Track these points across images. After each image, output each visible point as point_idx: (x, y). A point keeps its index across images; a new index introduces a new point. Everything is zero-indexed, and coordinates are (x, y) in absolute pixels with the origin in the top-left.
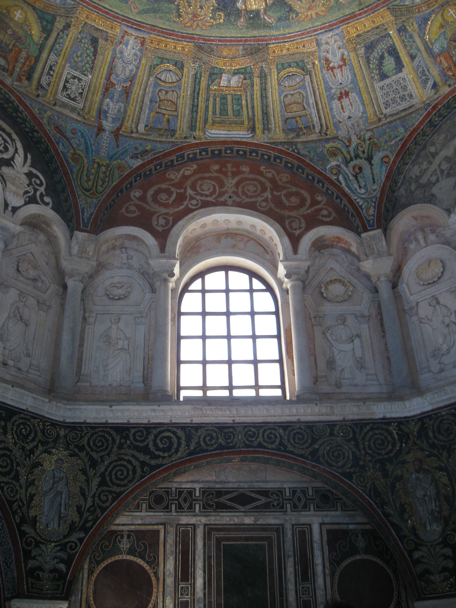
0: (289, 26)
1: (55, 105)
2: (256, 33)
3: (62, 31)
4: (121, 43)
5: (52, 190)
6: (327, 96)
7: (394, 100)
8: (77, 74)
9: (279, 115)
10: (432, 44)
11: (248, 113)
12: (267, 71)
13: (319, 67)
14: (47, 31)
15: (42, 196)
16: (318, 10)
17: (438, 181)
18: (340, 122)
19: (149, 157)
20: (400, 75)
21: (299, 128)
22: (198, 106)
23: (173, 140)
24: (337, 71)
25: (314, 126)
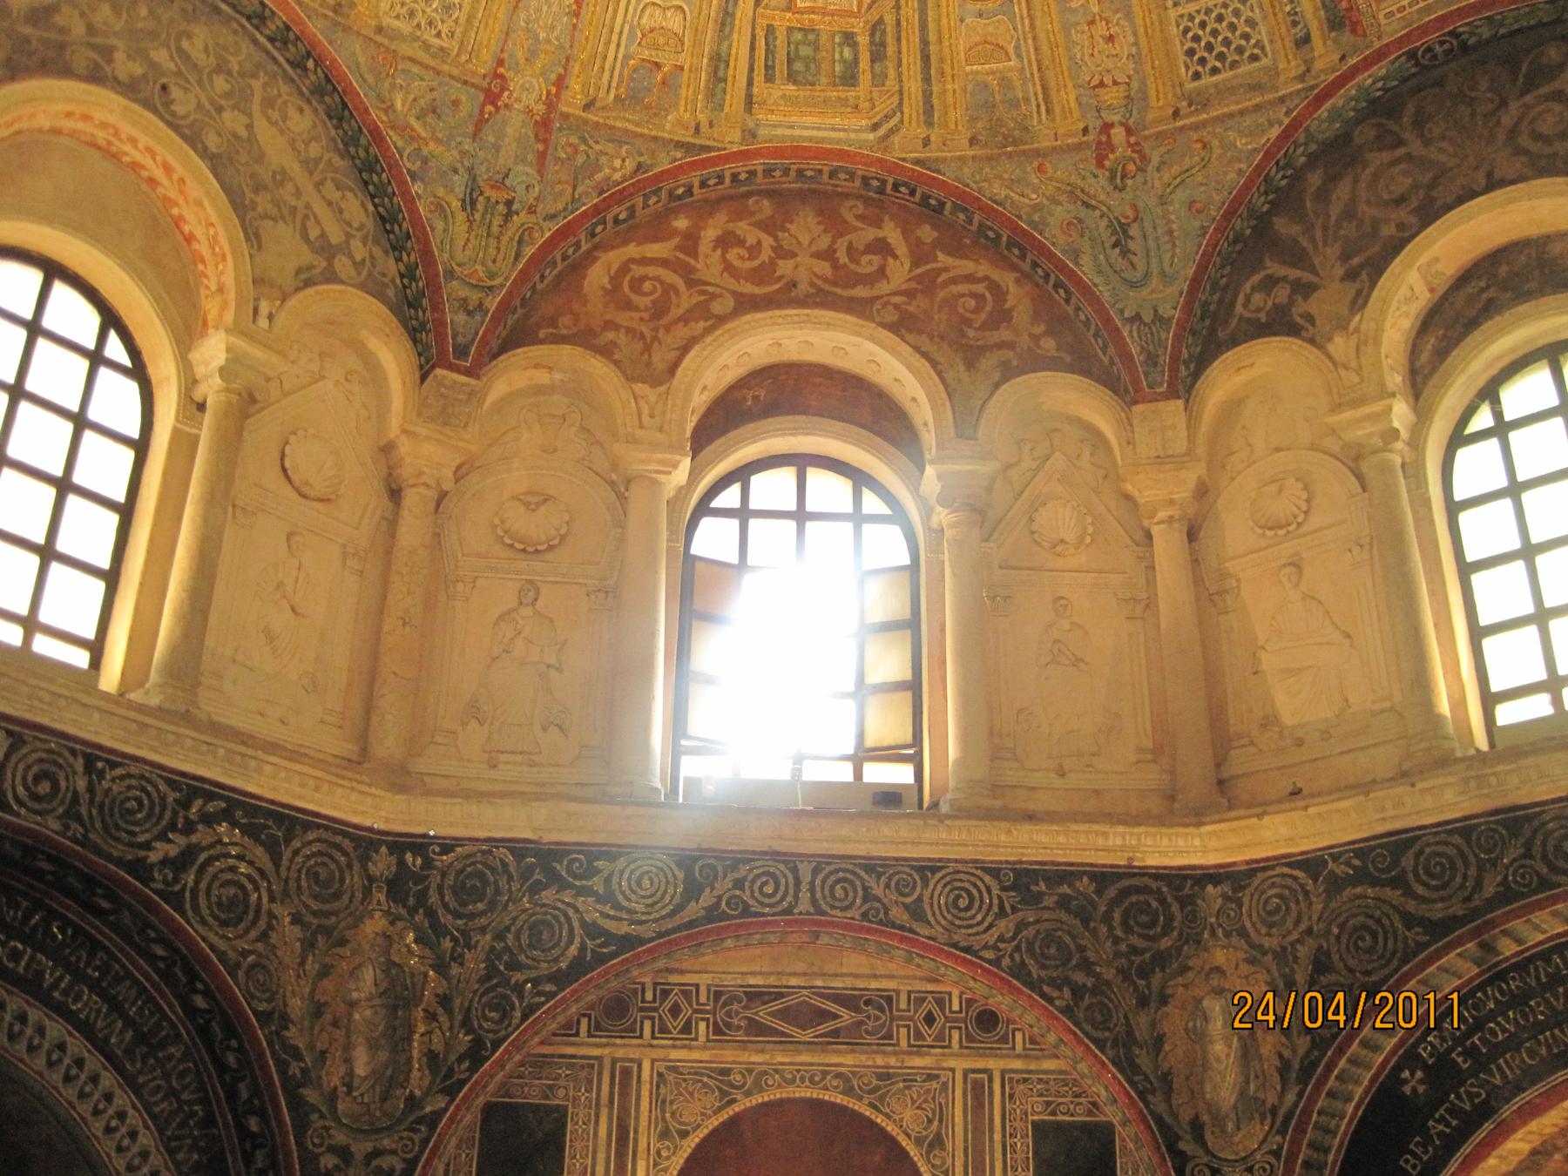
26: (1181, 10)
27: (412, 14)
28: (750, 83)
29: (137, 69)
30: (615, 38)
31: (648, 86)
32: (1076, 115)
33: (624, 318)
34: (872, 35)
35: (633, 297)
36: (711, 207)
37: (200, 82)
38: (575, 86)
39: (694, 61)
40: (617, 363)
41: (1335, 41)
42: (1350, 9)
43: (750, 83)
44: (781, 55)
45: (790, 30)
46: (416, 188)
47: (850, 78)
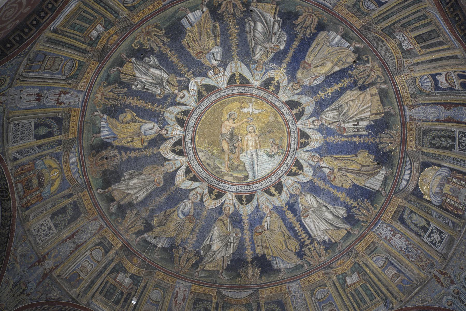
6: (44, 87)
7: (18, 130)
9: (52, 52)
10: (42, 160)
11: (68, 32)
12: (86, 55)
13: (66, 87)
16: (98, 99)
18: (21, 91)
21: (34, 62)
22: (99, 4)
24: (56, 97)
25: (29, 72)
27: (38, 231)
28: (96, 292)
30: (75, 264)
31: (74, 279)
34: (127, 295)
39: (87, 279)
43: (96, 292)
45: (112, 284)
47: (117, 303)
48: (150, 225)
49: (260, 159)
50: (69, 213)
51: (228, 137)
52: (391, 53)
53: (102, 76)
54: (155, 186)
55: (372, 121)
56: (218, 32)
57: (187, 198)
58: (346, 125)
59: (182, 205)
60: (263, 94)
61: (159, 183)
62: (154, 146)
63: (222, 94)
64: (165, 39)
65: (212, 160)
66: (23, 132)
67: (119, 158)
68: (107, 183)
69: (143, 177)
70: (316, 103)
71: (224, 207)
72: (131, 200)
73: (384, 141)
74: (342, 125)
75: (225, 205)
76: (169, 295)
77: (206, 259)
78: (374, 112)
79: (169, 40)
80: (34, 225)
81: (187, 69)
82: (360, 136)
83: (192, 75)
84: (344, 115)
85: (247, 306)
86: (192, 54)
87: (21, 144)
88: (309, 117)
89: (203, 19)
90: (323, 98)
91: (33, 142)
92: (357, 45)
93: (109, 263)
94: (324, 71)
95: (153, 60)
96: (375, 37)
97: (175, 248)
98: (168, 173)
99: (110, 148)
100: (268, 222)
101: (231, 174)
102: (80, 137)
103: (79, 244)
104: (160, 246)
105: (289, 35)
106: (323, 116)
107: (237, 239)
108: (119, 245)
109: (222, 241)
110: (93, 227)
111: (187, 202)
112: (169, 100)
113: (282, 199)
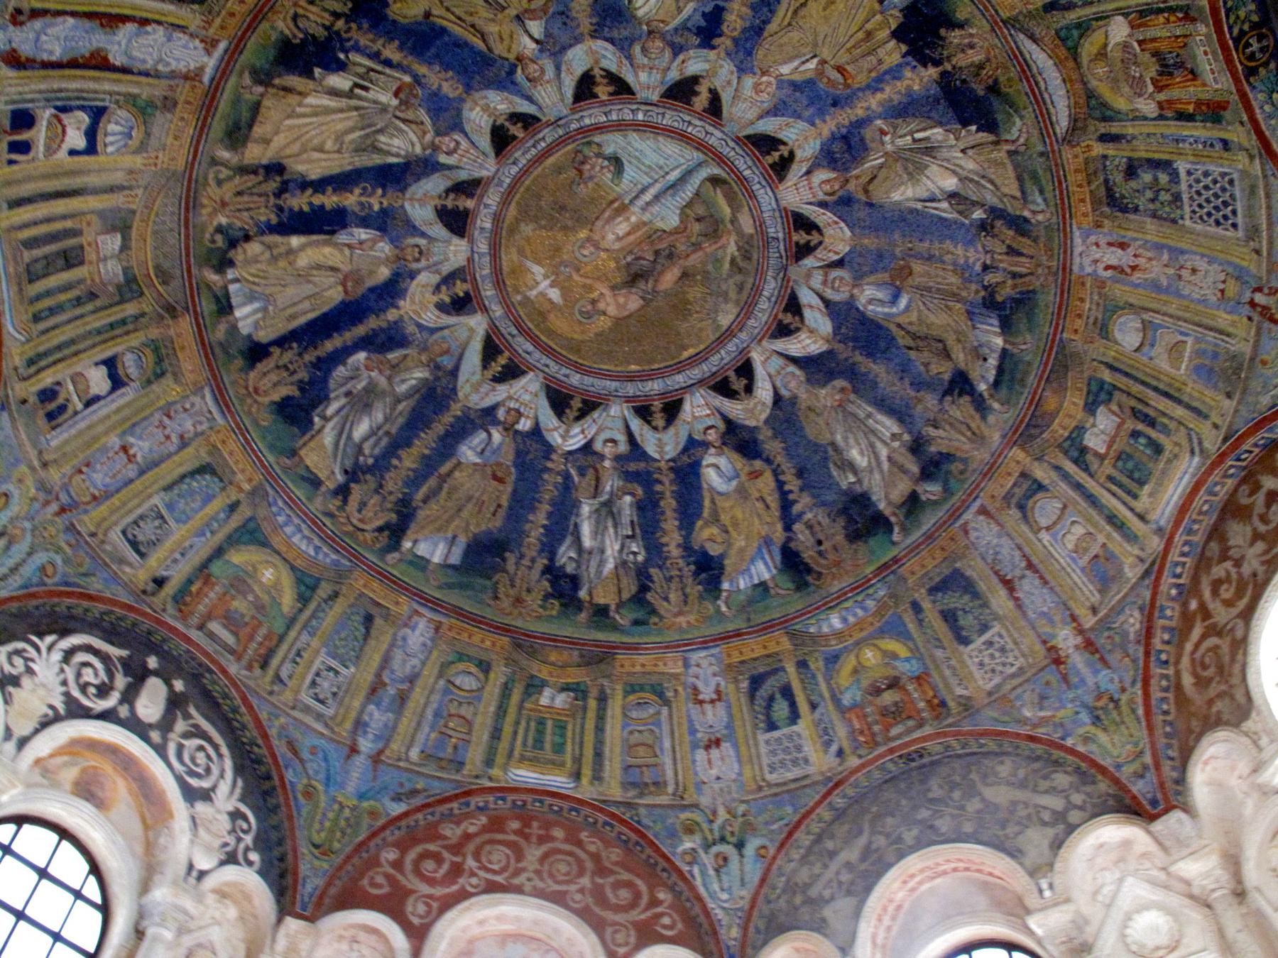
0: (648, 634)
1: (293, 708)
2: (601, 636)
3: (325, 601)
4: (406, 625)
5: (262, 843)
8: (334, 663)
14: (304, 600)
15: (247, 849)
16: (692, 618)
17: (832, 898)
19: (418, 801)
20: (795, 728)
23: (458, 777)
24: (708, 707)
25: (665, 783)
26: (1187, 216)
27: (993, 671)
29: (915, 832)
31: (1102, 570)
32: (1236, 318)
33: (1213, 690)
35: (1206, 674)
36: (1195, 579)
37: (947, 806)
38: (1082, 612)
40: (1227, 723)
41: (1229, 123)
42: (1208, 106)
43: (1132, 510)
44: (1125, 480)
46: (1069, 742)
47: (1158, 449)
48: (952, 382)
49: (646, 180)
50: (954, 600)
51: (642, 285)
52: (155, 233)
53: (640, 635)
54: (852, 397)
55: (313, 79)
56: (432, 482)
57: (850, 304)
58: (386, 98)
59: (875, 311)
60: (488, 292)
61: (843, 390)
62: (755, 441)
63: (554, 368)
64: (511, 558)
65: (724, 287)
66: (786, 751)
67: (809, 516)
68: (879, 523)
69: (839, 438)
70: (403, 190)
71: (827, 198)
72: (903, 450)
73: (326, 15)
74: (395, 102)
75: (821, 196)
76: (1120, 292)
77: (991, 199)
78: (293, 99)
79: (507, 554)
80: (981, 683)
81: (546, 476)
82: (375, 56)
83: (554, 457)
84: (369, 126)
85: (1070, 43)
86: (509, 489)
87: (811, 749)
88: (450, 168)
89: (426, 532)
90: (380, 191)
91: (803, 727)
92: (213, 277)
93: (1066, 476)
94: (327, 250)
95: (565, 555)
96: (165, 283)
97: (992, 295)
98: (808, 381)
99: (792, 545)
100: (796, 63)
101: (732, 222)
102: (784, 622)
103: (1024, 564)
104: (999, 342)
105: (328, 373)
106: (418, 150)
107: (895, 128)
108: (1017, 453)
109: (921, 168)
110: (984, 533)
111: (861, 302)
112: (632, 467)
113: (707, 66)
